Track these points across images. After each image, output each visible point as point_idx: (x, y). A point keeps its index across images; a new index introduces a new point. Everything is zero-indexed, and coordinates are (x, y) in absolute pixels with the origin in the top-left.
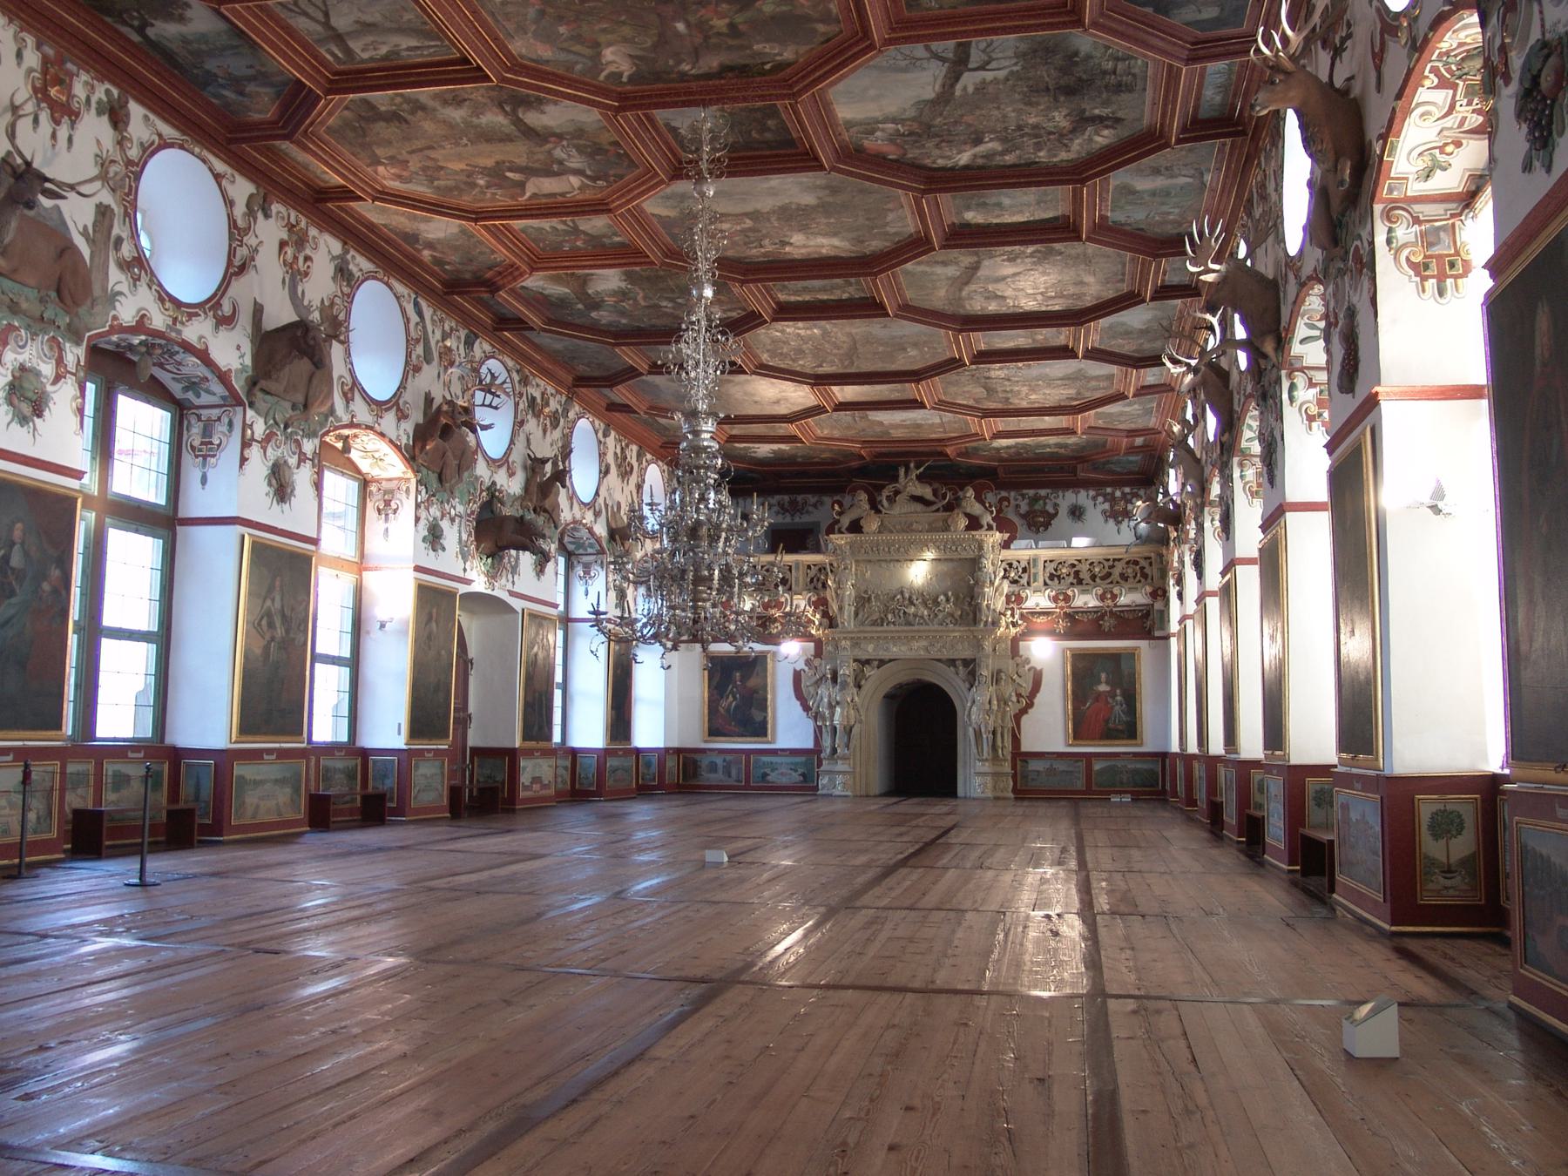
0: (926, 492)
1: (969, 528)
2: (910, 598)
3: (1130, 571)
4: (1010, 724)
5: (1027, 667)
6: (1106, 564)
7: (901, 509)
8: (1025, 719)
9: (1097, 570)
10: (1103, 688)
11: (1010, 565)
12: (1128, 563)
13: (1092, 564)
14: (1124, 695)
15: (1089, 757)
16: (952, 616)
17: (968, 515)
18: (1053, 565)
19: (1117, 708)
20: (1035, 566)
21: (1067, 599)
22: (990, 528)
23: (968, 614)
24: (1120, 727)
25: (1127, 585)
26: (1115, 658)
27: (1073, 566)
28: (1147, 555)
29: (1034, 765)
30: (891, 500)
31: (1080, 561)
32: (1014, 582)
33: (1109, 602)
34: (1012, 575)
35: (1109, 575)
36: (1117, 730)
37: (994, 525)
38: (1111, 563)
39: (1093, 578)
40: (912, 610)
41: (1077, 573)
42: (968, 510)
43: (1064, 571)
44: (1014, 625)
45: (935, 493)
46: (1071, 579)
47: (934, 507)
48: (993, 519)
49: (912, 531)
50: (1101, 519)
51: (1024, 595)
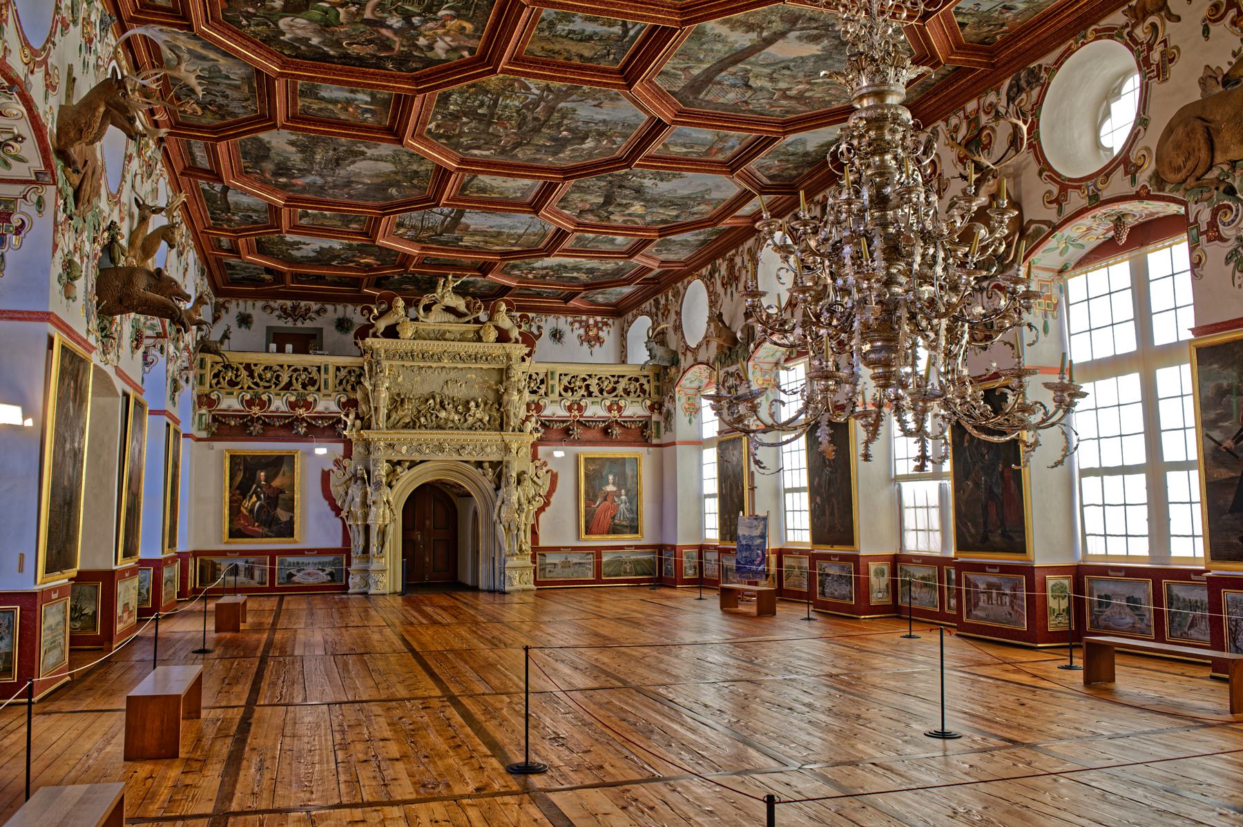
0: (460, 303)
1: (498, 340)
2: (442, 402)
3: (632, 386)
4: (531, 521)
5: (545, 469)
6: (612, 380)
7: (436, 320)
8: (542, 516)
9: (606, 384)
10: (610, 488)
11: (530, 376)
12: (630, 379)
13: (599, 379)
14: (626, 495)
15: (598, 551)
16: (481, 420)
17: (497, 328)
18: (568, 378)
19: (622, 506)
20: (552, 379)
21: (580, 409)
22: (517, 341)
23: (495, 421)
24: (624, 523)
25: (629, 399)
26: (621, 462)
27: (584, 380)
28: (646, 373)
29: (551, 559)
30: (428, 308)
31: (590, 376)
32: (533, 392)
33: (615, 413)
34: (532, 385)
35: (614, 389)
36: (623, 526)
37: (520, 339)
38: (616, 379)
39: (601, 391)
40: (443, 414)
41: (587, 387)
42: (501, 324)
43: (578, 383)
44: (536, 430)
45: (467, 307)
46: (583, 392)
47: (467, 319)
48: (520, 333)
49: (446, 340)
50: (578, 342)
51: (541, 403)
